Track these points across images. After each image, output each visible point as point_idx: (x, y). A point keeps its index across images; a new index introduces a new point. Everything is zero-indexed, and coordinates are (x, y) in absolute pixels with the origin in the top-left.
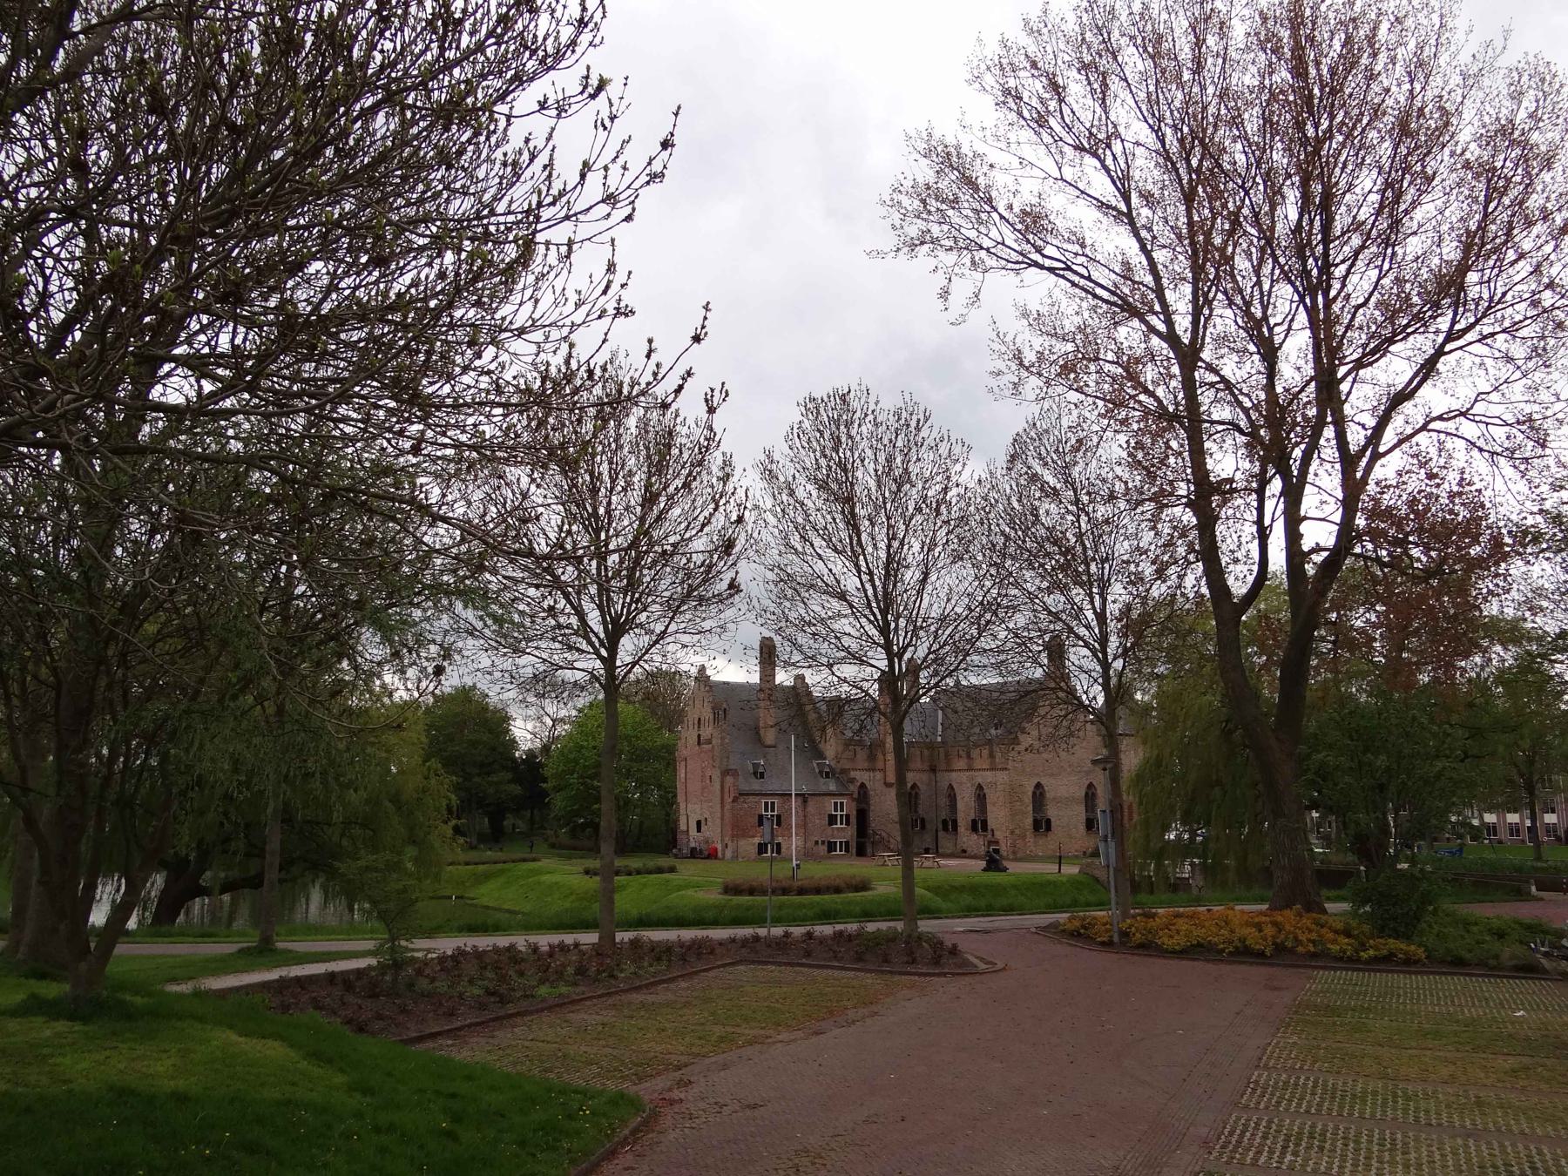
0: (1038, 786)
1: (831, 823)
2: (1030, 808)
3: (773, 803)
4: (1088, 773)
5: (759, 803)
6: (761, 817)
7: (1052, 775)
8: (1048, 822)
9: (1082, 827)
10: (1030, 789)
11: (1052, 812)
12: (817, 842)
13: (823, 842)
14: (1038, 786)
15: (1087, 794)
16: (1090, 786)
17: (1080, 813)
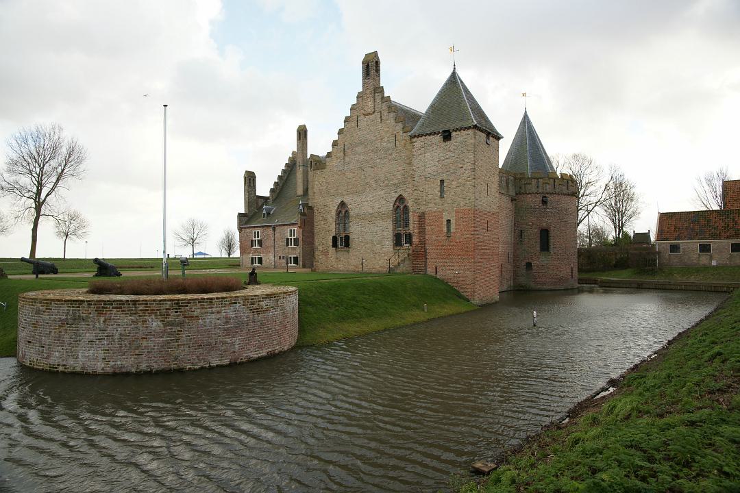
0: (343, 204)
1: (287, 245)
2: (333, 227)
3: (258, 232)
4: (397, 186)
5: (251, 232)
6: (252, 241)
7: (356, 193)
8: (347, 238)
9: (388, 245)
10: (333, 209)
11: (355, 230)
12: (280, 257)
13: (283, 257)
14: (343, 204)
15: (396, 209)
16: (401, 199)
17: (386, 229)
